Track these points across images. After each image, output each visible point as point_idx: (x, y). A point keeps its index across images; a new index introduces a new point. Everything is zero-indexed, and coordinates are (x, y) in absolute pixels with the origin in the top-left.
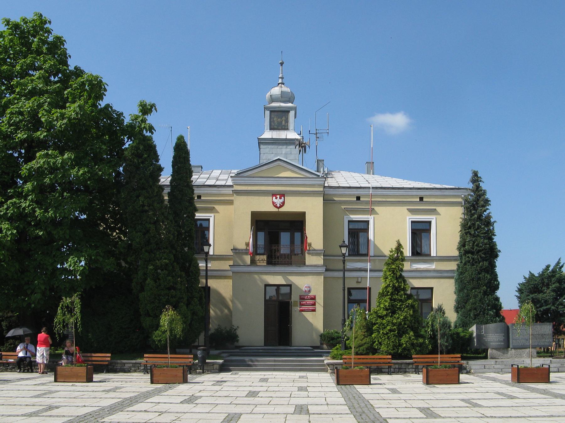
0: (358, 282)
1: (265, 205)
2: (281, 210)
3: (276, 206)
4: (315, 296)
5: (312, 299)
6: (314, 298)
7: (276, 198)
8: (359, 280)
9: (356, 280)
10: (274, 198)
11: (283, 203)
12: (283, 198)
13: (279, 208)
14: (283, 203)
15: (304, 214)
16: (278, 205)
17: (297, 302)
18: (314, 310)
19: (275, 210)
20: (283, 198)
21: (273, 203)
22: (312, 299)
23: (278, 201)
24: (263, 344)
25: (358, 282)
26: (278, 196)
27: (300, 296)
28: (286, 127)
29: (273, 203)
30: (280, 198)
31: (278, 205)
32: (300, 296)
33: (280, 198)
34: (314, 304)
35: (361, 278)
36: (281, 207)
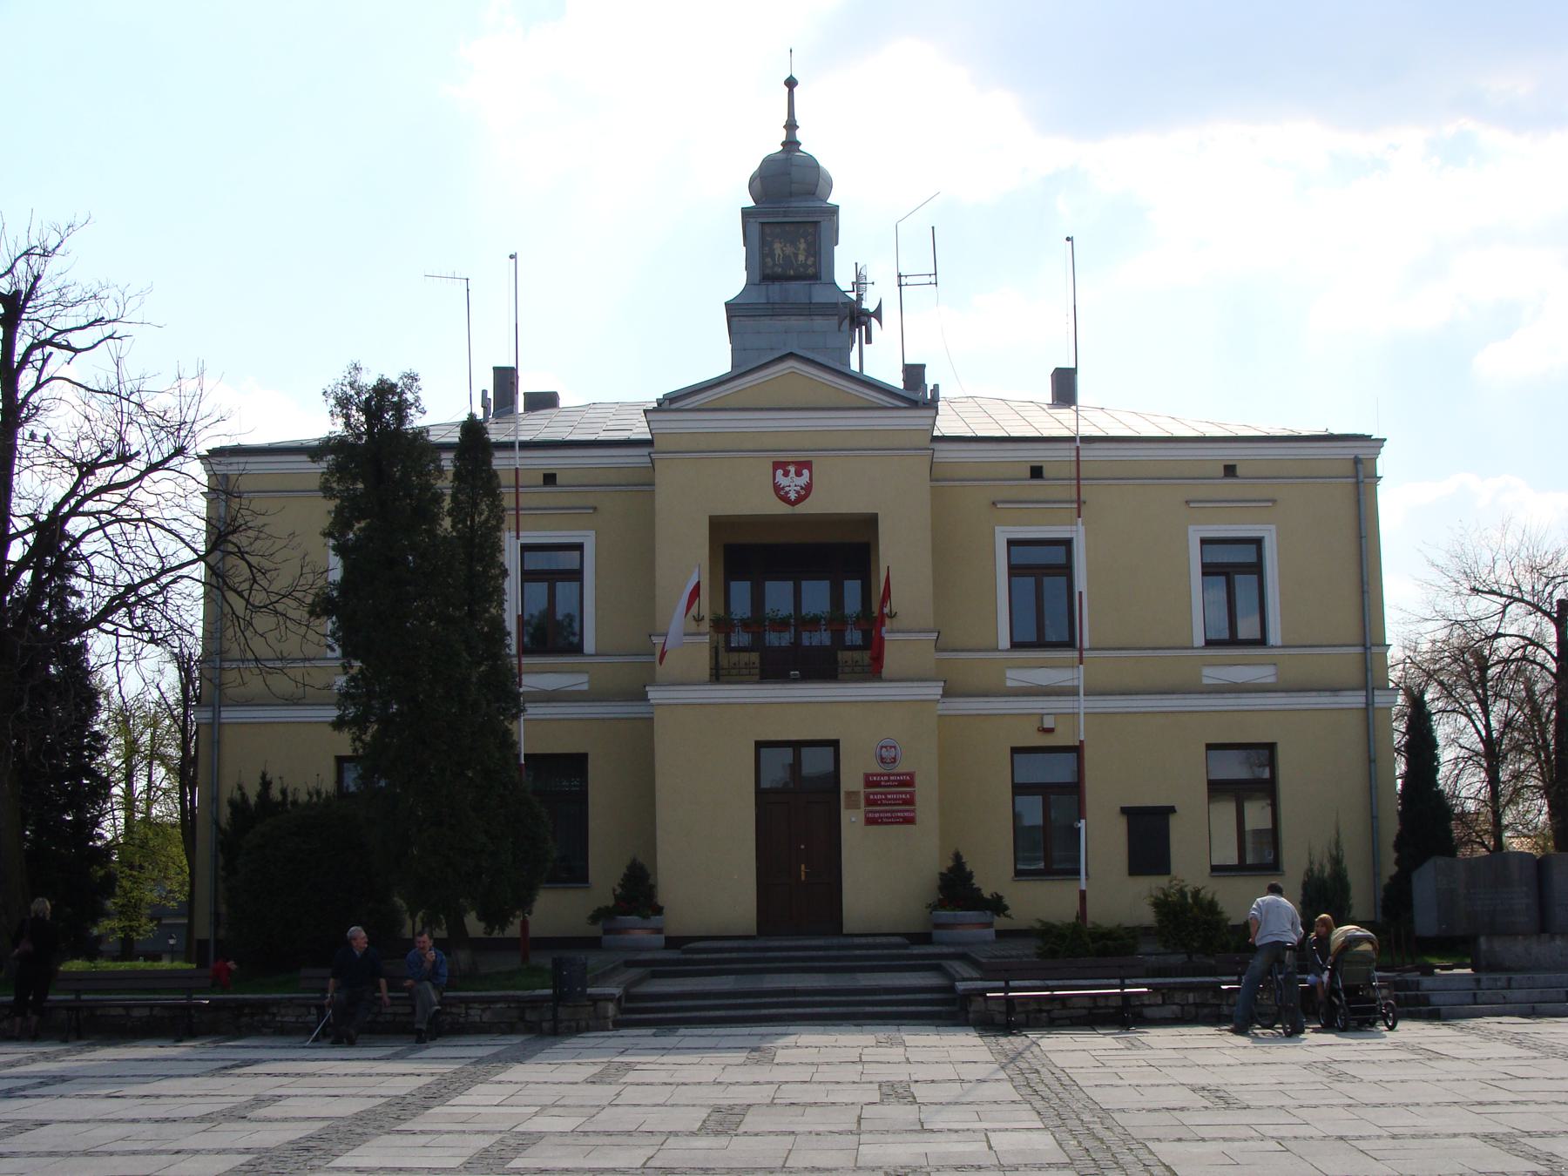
2: (801, 509)
3: (785, 499)
4: (911, 775)
5: (902, 784)
6: (908, 781)
7: (786, 474)
10: (780, 472)
11: (808, 488)
12: (806, 472)
15: (871, 522)
16: (793, 496)
17: (856, 793)
18: (910, 821)
19: (782, 509)
20: (806, 472)
22: (902, 784)
23: (792, 483)
24: (753, 930)
26: (792, 469)
27: (867, 776)
28: (811, 271)
29: (777, 489)
30: (799, 474)
31: (793, 496)
32: (867, 776)
33: (799, 474)
34: (910, 802)
36: (800, 499)
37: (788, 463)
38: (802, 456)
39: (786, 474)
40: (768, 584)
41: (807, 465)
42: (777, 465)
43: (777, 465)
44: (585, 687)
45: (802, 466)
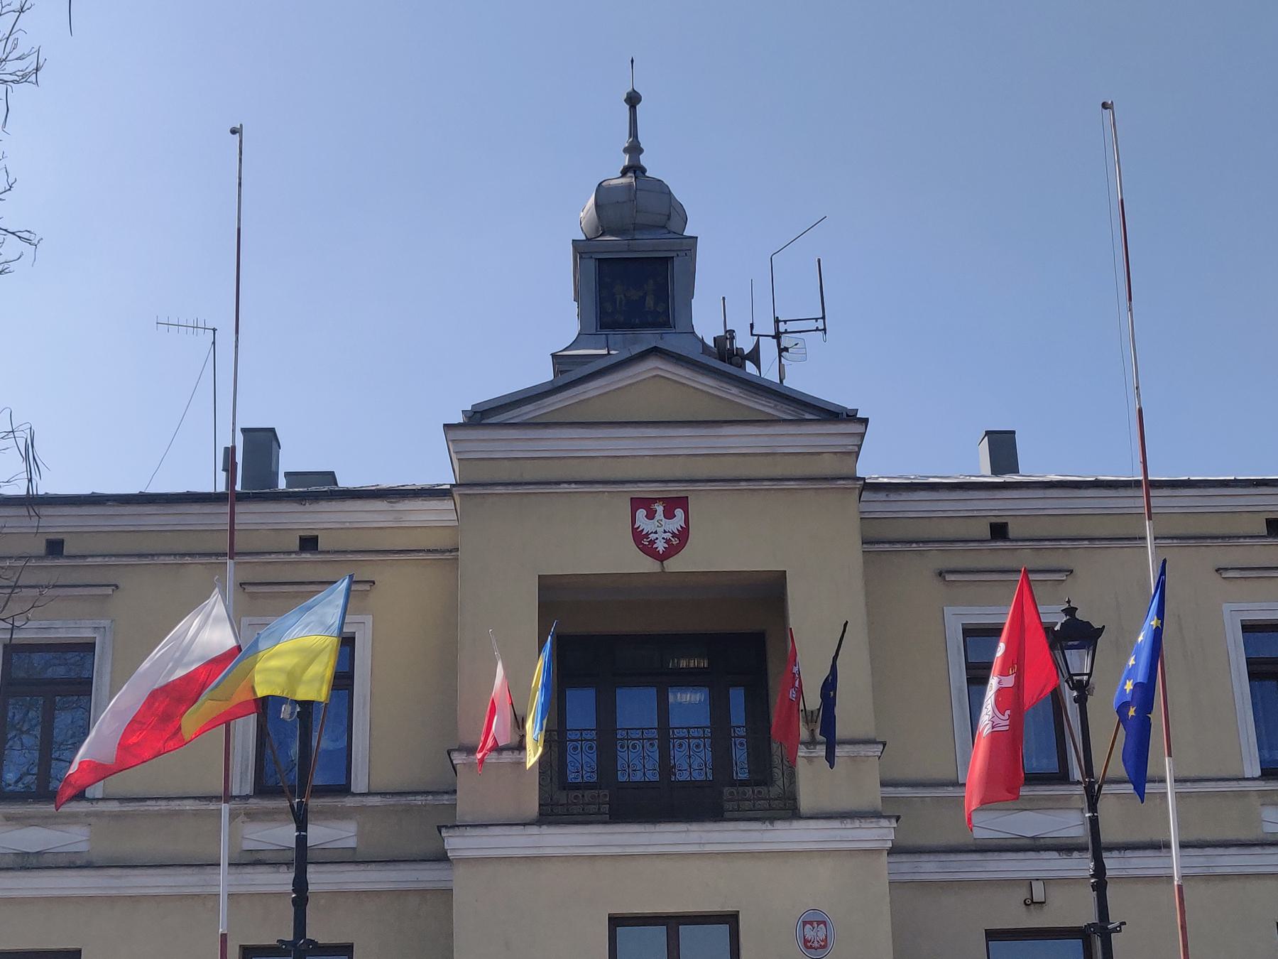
0: (1030, 903)
1: (601, 546)
7: (651, 515)
8: (1038, 895)
9: (1024, 894)
10: (641, 513)
11: (683, 535)
12: (679, 512)
13: (661, 558)
14: (683, 535)
16: (661, 546)
19: (647, 565)
20: (679, 512)
21: (638, 536)
23: (660, 527)
25: (1030, 903)
26: (659, 508)
29: (638, 536)
30: (669, 515)
31: (661, 546)
33: (669, 515)
35: (1046, 881)
37: (655, 500)
38: (675, 490)
39: (651, 515)
40: (620, 693)
41: (682, 502)
42: (637, 503)
43: (637, 503)
44: (352, 843)
45: (674, 504)
